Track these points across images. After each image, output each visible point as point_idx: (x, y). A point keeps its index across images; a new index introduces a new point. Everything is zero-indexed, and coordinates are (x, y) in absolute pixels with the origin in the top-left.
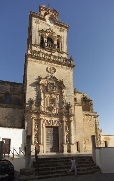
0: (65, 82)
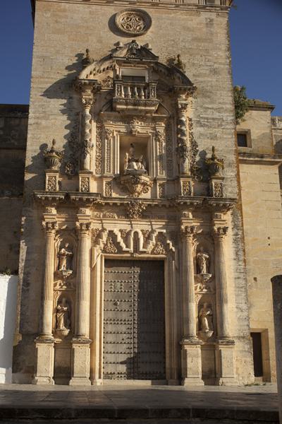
0: (194, 64)
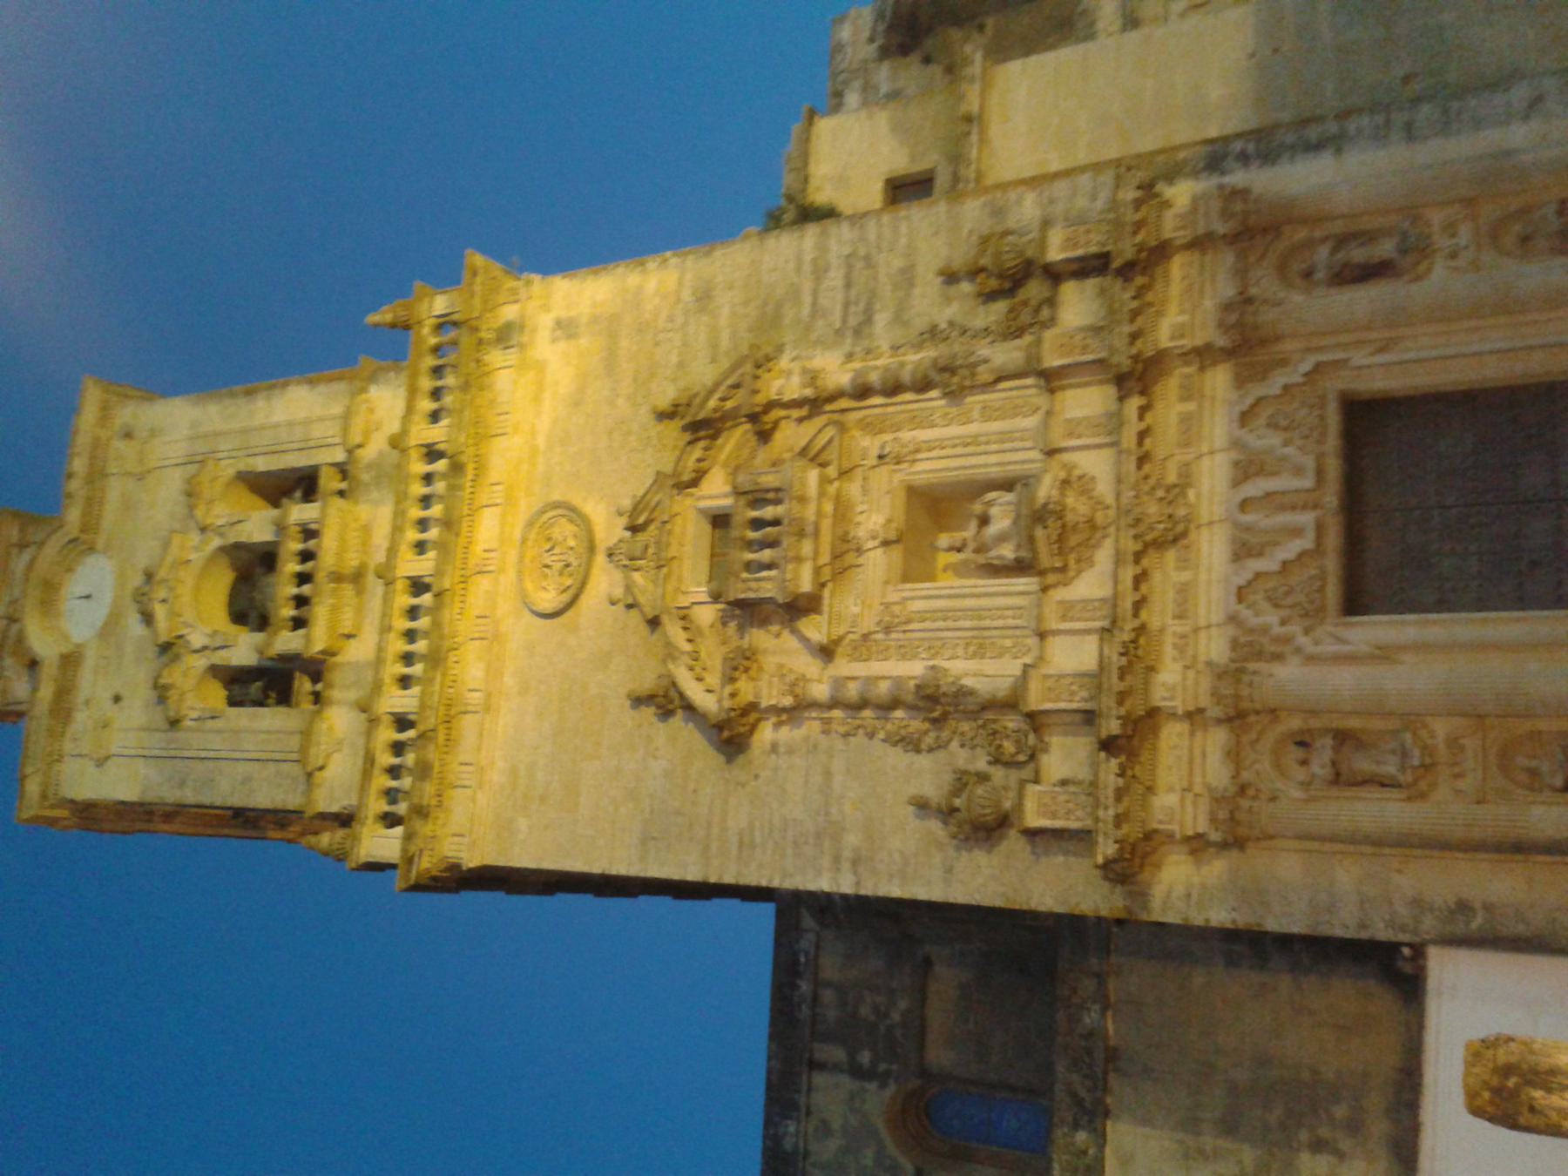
0: (681, 365)
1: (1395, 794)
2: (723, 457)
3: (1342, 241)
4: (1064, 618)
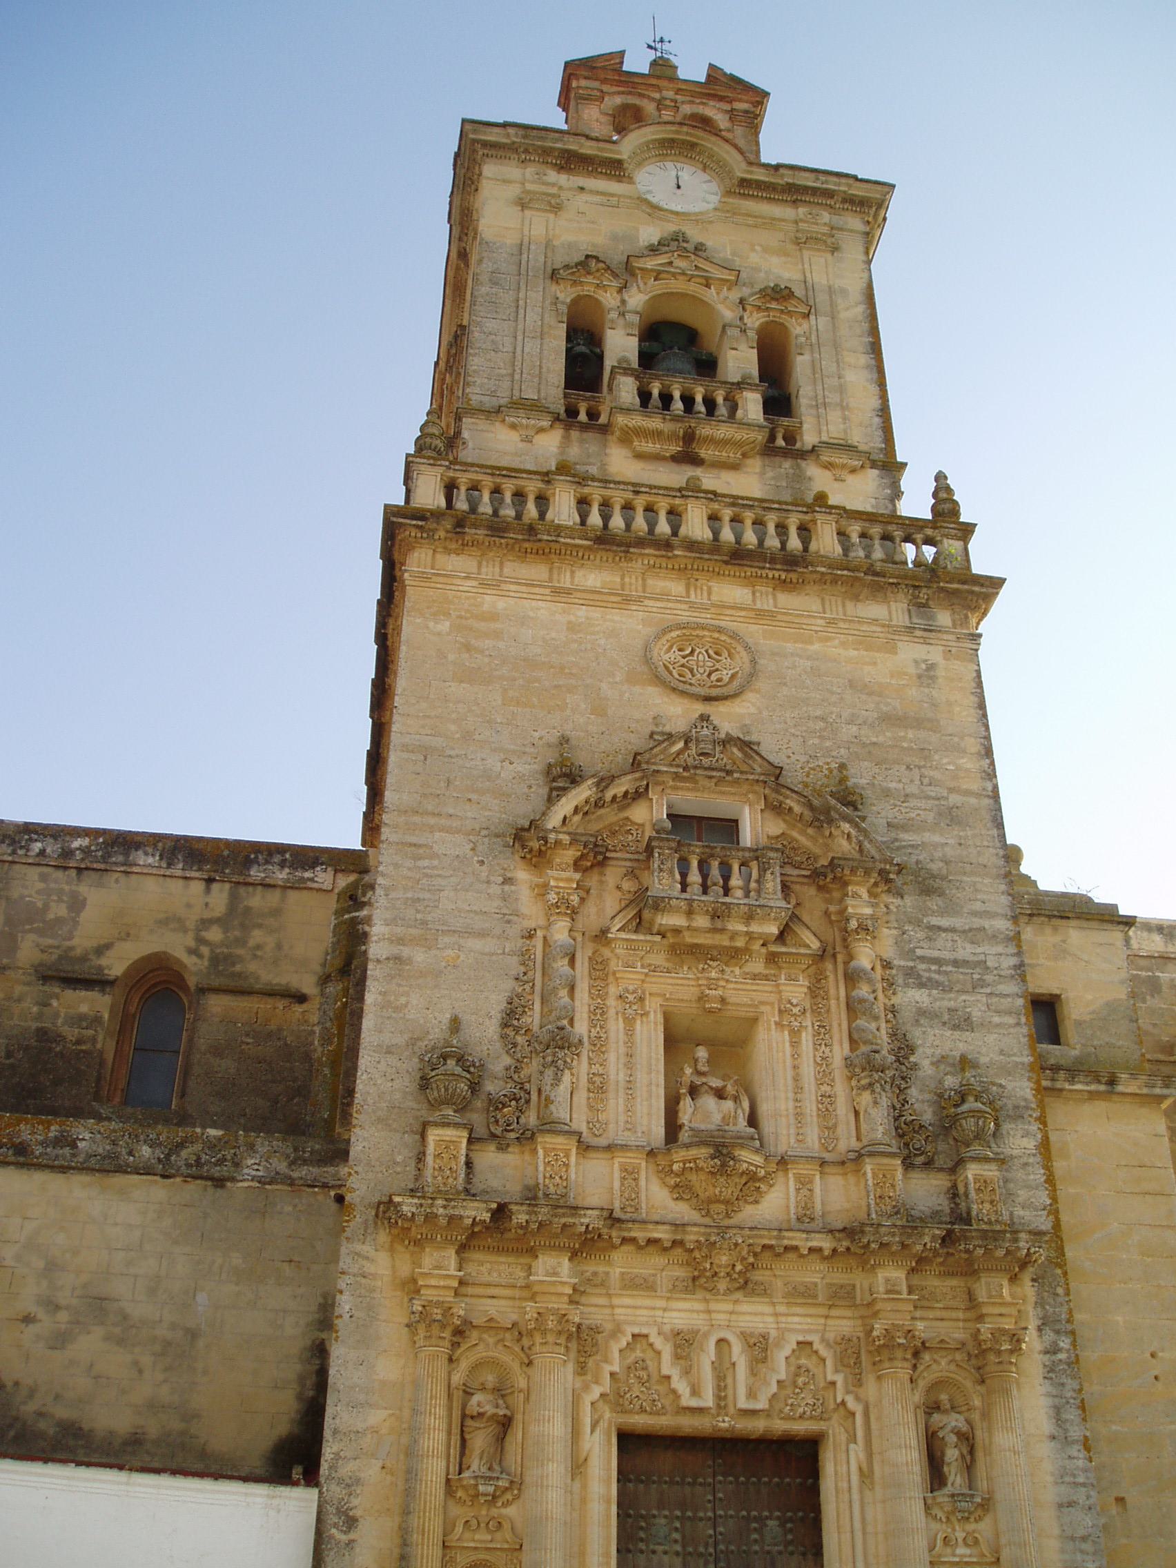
0: (887, 793)
1: (454, 1468)
2: (795, 834)
3: (967, 1439)
4: (624, 1169)
